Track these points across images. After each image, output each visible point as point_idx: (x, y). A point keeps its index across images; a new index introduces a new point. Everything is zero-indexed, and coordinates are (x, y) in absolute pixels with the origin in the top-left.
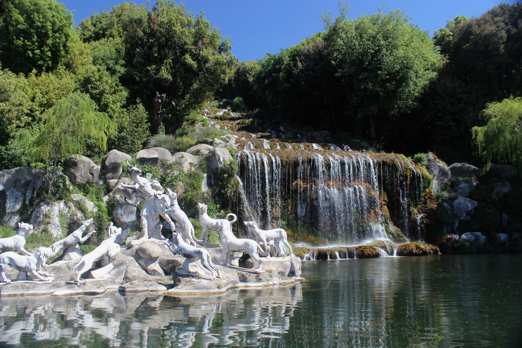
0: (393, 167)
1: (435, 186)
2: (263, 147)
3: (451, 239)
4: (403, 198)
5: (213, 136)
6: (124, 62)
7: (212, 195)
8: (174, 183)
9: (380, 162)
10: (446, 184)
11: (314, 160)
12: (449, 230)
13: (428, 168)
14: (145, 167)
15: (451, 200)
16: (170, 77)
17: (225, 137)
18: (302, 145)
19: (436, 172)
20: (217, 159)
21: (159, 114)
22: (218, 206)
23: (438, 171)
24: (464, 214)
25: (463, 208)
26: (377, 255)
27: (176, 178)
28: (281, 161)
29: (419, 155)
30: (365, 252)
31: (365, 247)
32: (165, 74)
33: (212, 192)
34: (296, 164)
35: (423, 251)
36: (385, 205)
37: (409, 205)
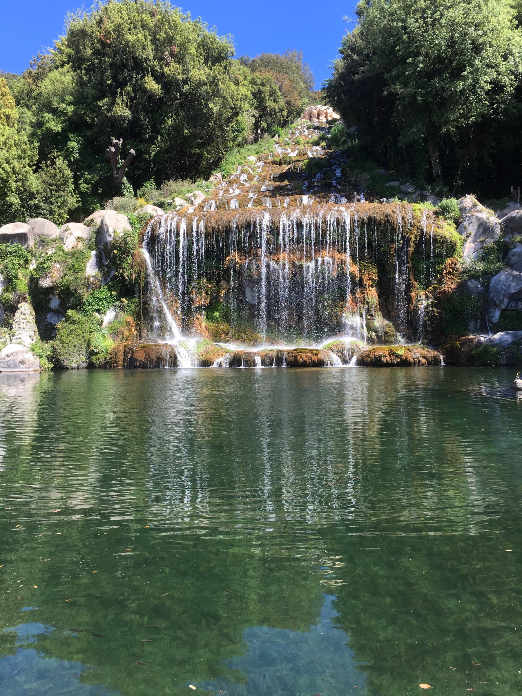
0: (384, 227)
1: (467, 255)
2: (229, 208)
3: (472, 340)
4: (401, 274)
5: (176, 194)
6: (71, 97)
7: (106, 279)
8: (45, 266)
9: (363, 219)
10: (489, 249)
11: (255, 223)
12: (478, 326)
13: (458, 223)
14: (8, 246)
15: (488, 275)
16: (128, 113)
17: (189, 195)
18: (287, 200)
19: (472, 229)
20: (106, 230)
21: (119, 168)
22: (114, 293)
23: (476, 227)
24: (506, 301)
25: (502, 288)
26: (321, 363)
27: (49, 259)
28: (206, 228)
29: (444, 202)
30: (299, 358)
31: (301, 351)
32: (121, 110)
33: (103, 275)
34: (228, 231)
35: (401, 359)
36: (372, 287)
37: (409, 287)
